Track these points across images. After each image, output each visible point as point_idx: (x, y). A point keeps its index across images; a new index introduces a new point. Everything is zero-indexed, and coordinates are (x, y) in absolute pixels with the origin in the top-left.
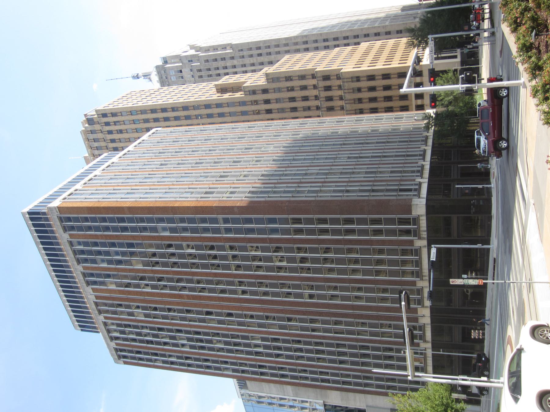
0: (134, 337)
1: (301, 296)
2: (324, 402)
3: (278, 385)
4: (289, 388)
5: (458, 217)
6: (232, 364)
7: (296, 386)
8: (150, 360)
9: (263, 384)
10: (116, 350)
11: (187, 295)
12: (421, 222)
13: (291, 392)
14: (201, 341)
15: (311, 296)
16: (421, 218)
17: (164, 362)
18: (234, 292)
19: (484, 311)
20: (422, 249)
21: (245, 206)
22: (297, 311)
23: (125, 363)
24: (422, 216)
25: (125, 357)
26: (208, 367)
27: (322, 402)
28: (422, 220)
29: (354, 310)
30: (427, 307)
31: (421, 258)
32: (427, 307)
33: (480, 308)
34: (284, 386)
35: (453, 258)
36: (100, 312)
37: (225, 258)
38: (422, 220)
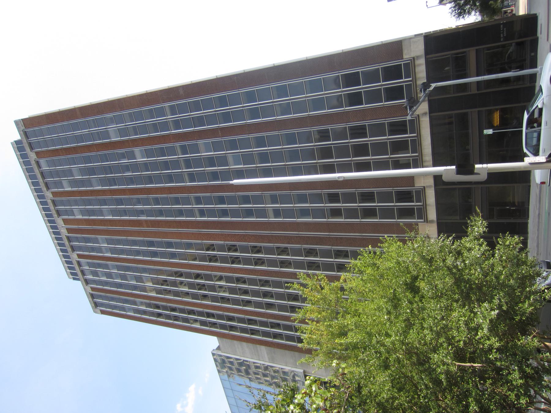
0: (186, 289)
1: (262, 213)
2: (304, 372)
3: (250, 345)
4: (263, 349)
5: (477, 51)
6: (201, 314)
7: (270, 346)
8: (186, 320)
9: (235, 342)
10: (92, 296)
11: (146, 221)
12: (417, 69)
13: (266, 356)
14: (246, 292)
15: (277, 213)
16: (417, 62)
17: (203, 323)
18: (190, 213)
19: (527, 224)
20: (421, 119)
21: (479, 22)
22: (320, 238)
23: (103, 312)
24: (418, 57)
25: (102, 305)
26: (176, 318)
27: (302, 371)
28: (419, 65)
29: (330, 232)
30: (432, 222)
31: (419, 136)
32: (432, 222)
33: (523, 221)
34: (258, 346)
35: (470, 131)
36: (73, 249)
37: (176, 164)
38: (419, 65)
